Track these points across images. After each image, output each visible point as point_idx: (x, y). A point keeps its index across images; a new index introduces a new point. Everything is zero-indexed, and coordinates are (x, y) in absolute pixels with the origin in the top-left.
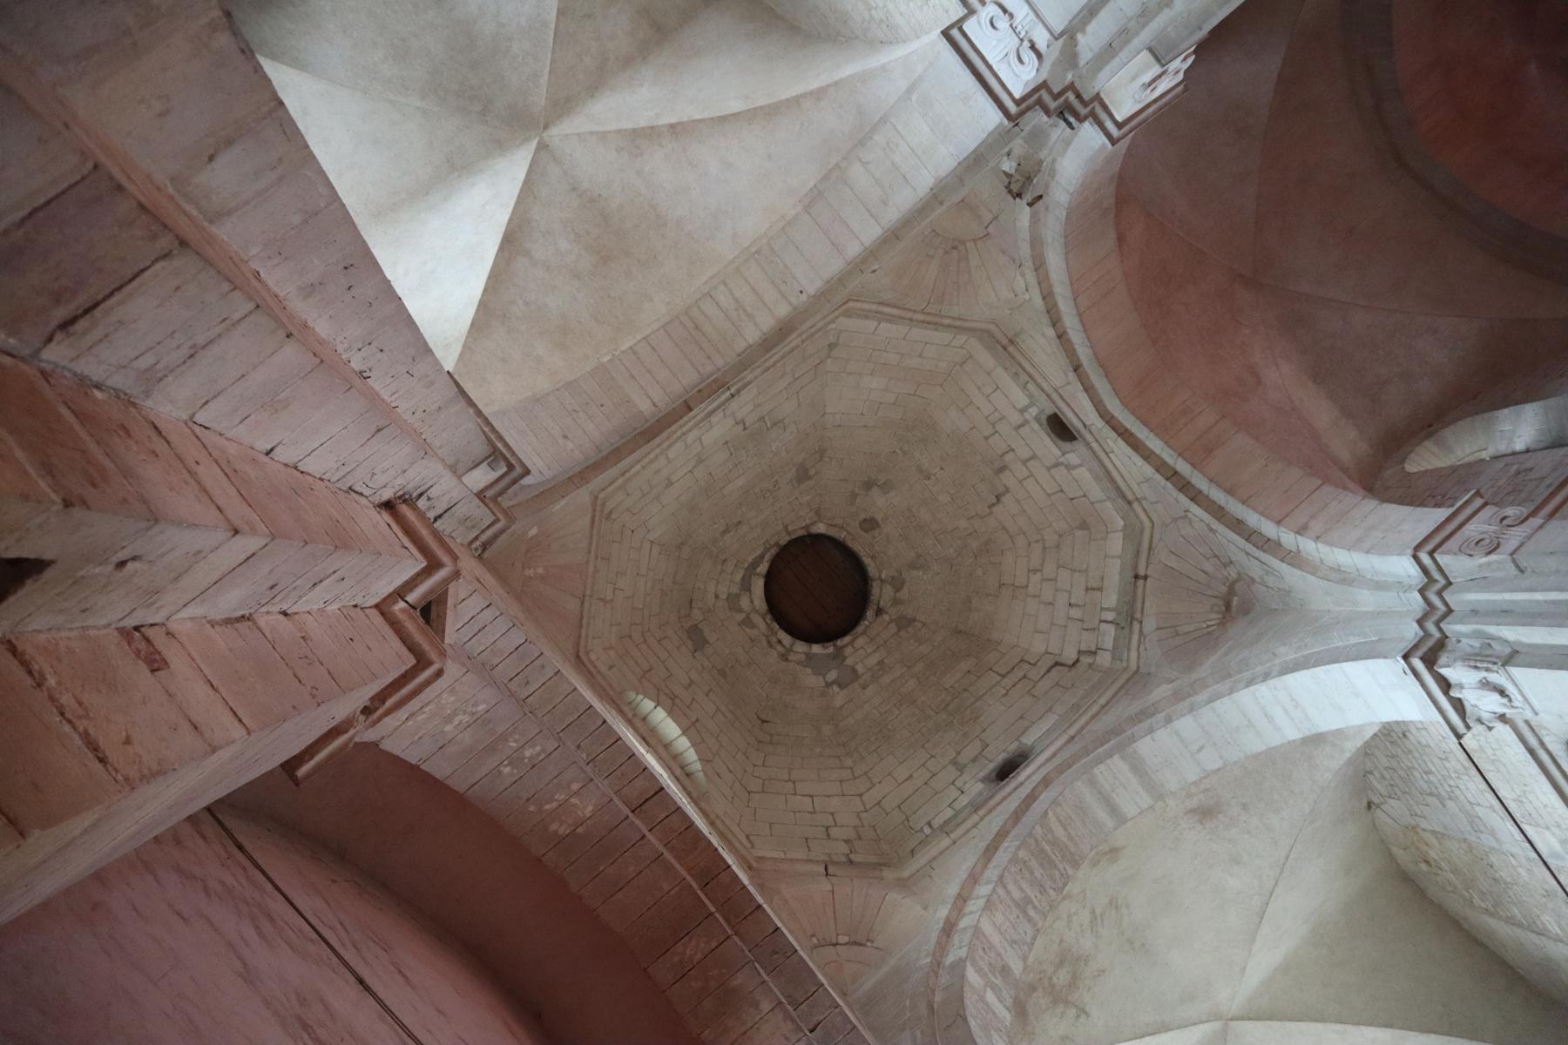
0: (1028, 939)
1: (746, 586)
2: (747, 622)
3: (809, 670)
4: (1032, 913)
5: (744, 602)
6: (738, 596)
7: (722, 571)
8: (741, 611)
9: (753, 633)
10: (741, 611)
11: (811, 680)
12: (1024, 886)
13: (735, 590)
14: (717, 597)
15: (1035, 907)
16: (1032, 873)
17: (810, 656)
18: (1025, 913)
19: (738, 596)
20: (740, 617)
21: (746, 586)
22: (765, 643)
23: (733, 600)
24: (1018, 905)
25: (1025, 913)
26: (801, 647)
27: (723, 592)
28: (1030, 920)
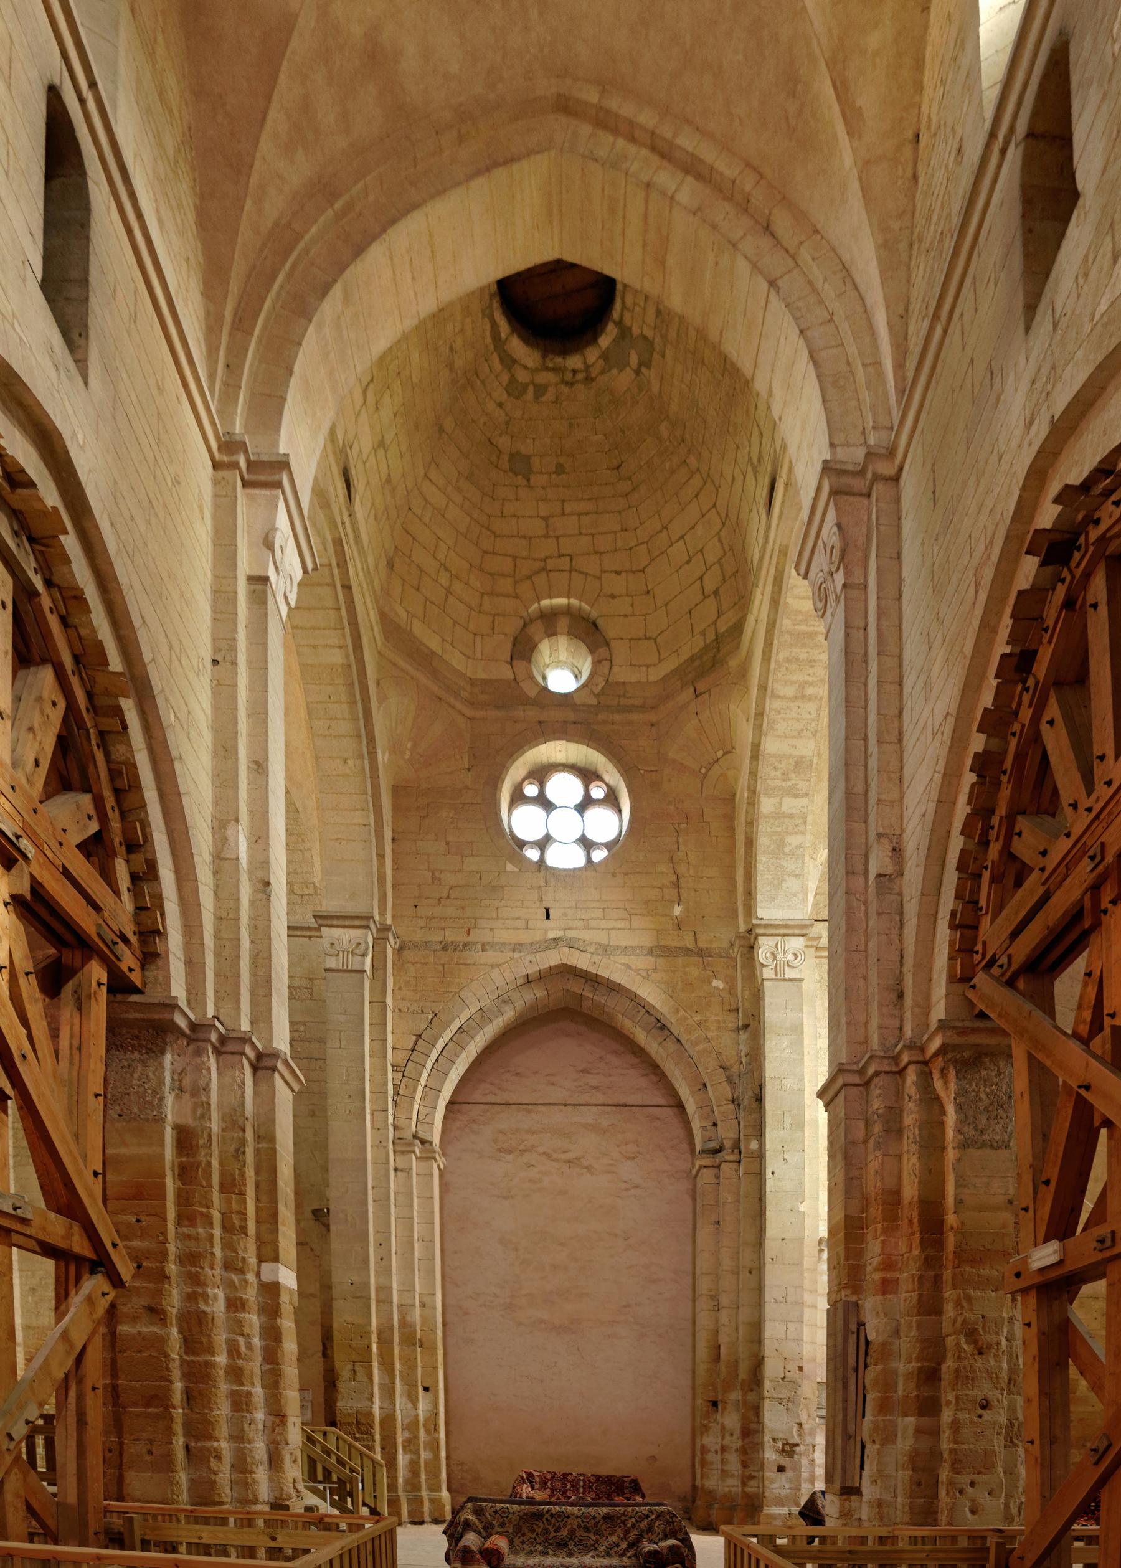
0: (814, 716)
1: (509, 362)
2: (540, 390)
3: (614, 371)
4: (810, 691)
5: (522, 376)
6: (513, 380)
7: (483, 382)
8: (525, 387)
9: (549, 396)
10: (525, 387)
11: (623, 379)
12: (795, 678)
13: (505, 378)
14: (501, 405)
15: (811, 684)
16: (797, 660)
17: (605, 356)
18: (803, 697)
19: (513, 380)
20: (530, 394)
21: (509, 362)
22: (565, 389)
23: (515, 390)
24: (796, 698)
25: (803, 697)
26: (592, 355)
27: (500, 394)
28: (810, 699)
